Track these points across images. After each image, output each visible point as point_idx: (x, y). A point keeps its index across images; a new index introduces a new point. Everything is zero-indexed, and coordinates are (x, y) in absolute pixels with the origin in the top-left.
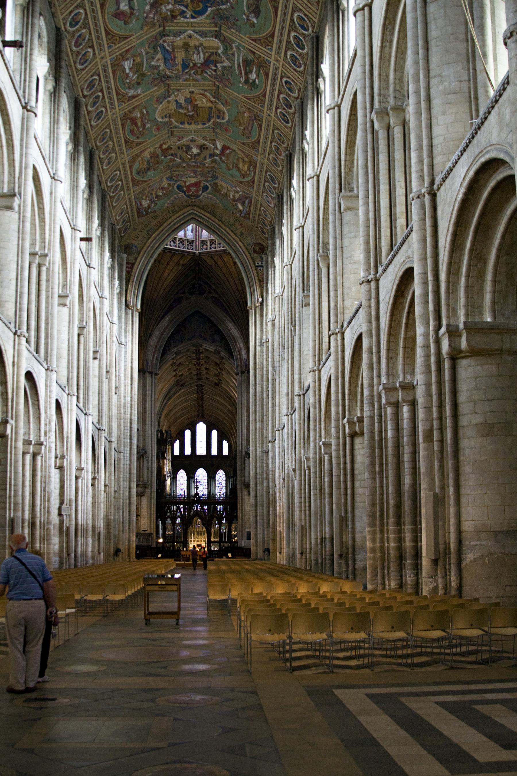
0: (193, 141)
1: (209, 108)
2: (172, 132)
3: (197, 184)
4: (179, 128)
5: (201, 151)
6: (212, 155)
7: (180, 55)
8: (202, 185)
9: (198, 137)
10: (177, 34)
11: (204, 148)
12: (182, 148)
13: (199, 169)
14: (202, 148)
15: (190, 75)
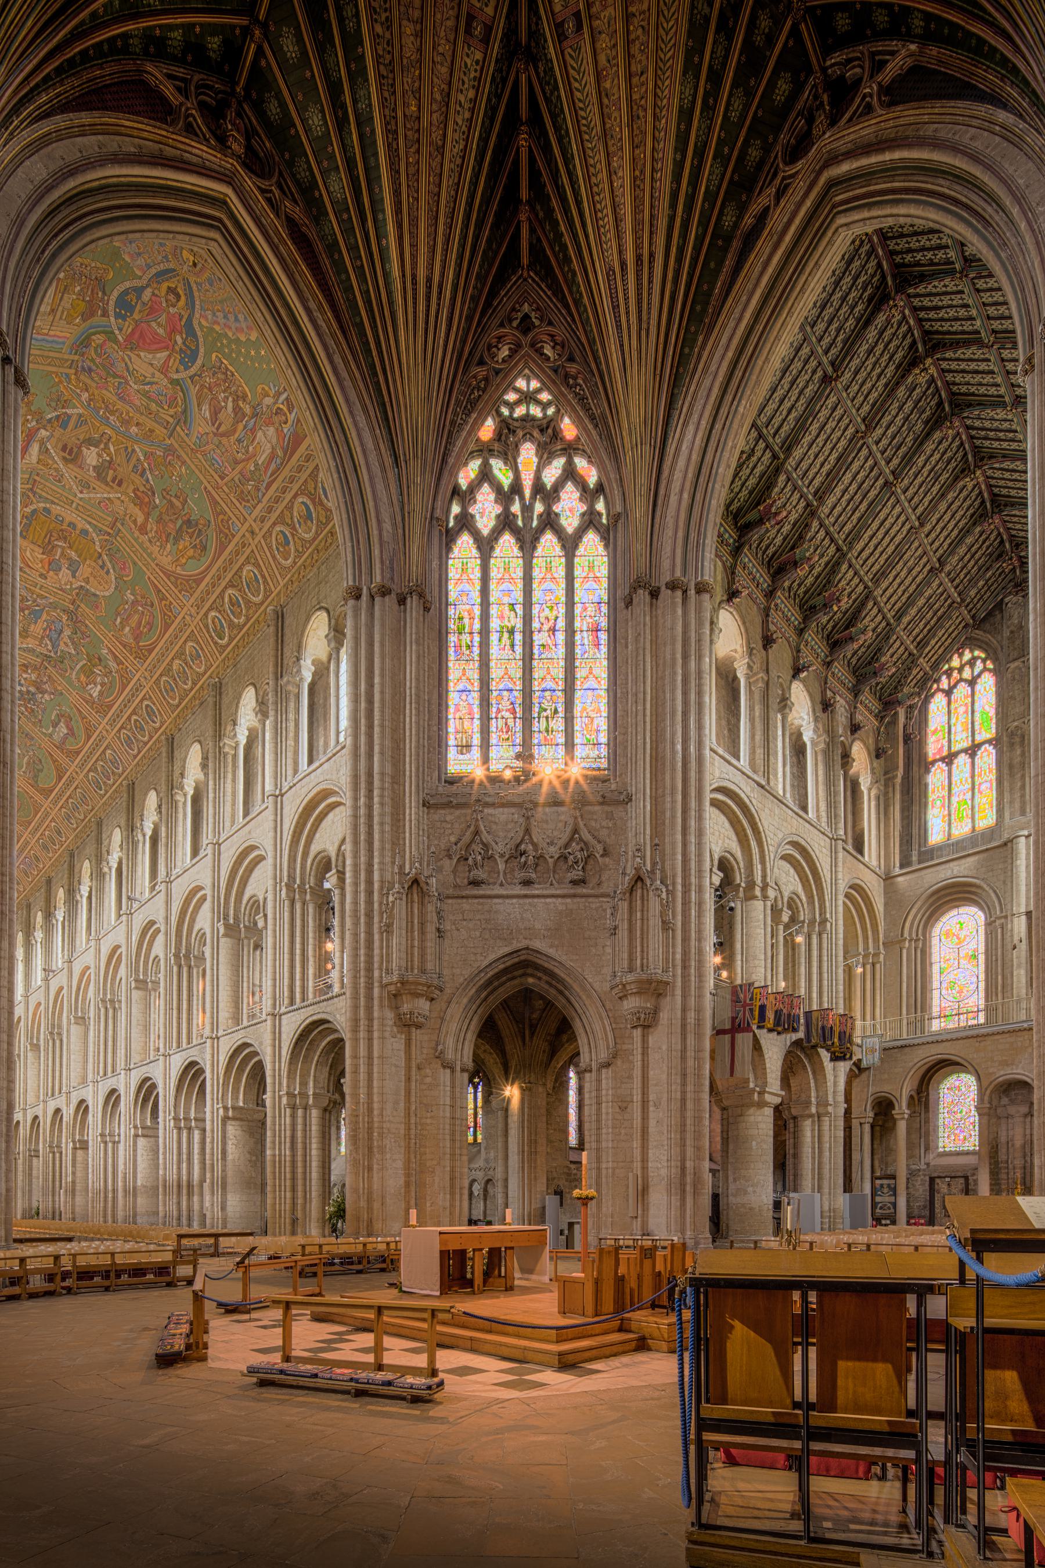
0: (85, 486)
1: (25, 538)
2: (113, 526)
3: (137, 341)
4: (95, 527)
5: (79, 448)
6: (63, 421)
7: (37, 629)
8: (128, 327)
9: (71, 489)
10: (32, 651)
11: (70, 454)
12: (113, 481)
13: (110, 396)
14: (72, 455)
15: (35, 601)
